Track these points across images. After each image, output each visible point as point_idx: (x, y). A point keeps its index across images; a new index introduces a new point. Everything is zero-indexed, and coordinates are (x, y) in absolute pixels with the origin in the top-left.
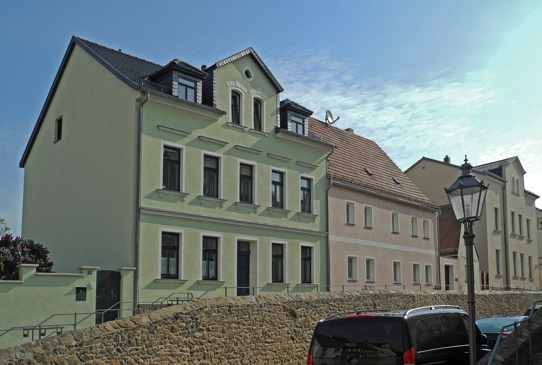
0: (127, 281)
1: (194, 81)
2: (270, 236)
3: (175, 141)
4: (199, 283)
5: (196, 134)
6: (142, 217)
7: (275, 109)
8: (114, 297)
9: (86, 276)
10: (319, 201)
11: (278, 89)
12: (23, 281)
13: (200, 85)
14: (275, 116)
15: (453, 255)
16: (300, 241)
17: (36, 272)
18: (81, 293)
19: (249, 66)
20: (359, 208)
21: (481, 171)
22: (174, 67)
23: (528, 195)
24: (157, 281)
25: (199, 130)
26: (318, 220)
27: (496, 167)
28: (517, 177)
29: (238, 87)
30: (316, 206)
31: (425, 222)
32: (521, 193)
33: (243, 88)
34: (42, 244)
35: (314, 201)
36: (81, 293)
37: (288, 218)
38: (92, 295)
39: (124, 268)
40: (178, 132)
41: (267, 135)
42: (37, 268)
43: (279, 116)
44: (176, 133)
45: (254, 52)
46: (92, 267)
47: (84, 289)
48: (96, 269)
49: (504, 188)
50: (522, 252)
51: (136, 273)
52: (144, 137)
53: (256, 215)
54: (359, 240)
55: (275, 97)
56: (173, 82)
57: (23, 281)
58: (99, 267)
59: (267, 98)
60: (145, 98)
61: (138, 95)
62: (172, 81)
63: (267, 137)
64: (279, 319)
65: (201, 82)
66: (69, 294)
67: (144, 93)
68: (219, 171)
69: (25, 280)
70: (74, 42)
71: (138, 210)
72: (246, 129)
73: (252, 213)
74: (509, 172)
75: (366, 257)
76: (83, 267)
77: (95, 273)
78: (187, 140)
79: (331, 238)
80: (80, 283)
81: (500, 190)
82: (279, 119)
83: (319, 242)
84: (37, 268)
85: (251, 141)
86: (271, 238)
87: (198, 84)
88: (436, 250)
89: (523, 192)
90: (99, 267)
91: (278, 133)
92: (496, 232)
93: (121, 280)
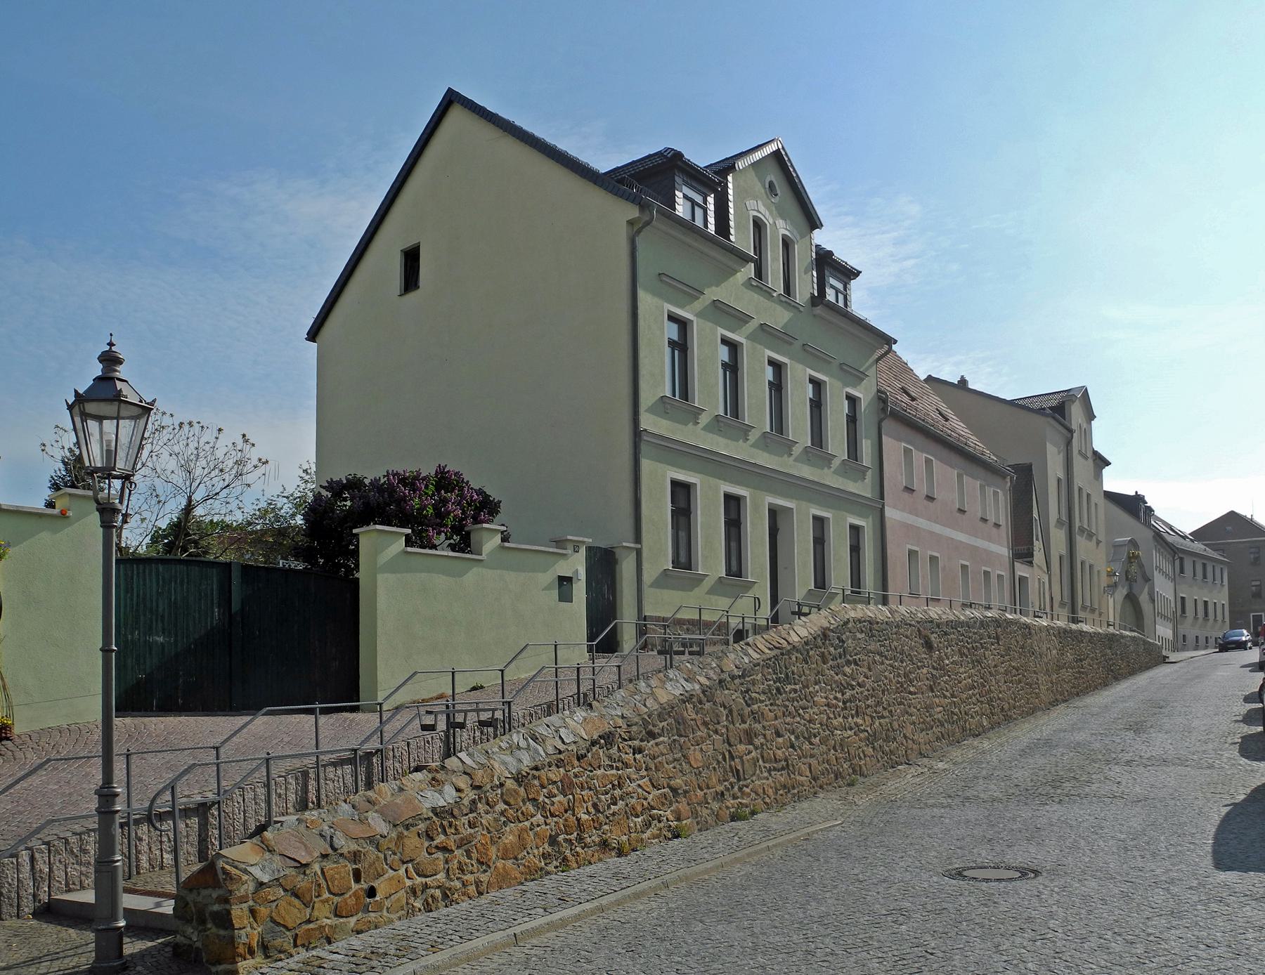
0: (626, 568)
1: (703, 193)
2: (810, 501)
3: (682, 307)
4: (721, 582)
5: (712, 293)
6: (644, 448)
7: (809, 260)
8: (609, 598)
9: (572, 555)
10: (869, 442)
11: (813, 222)
12: (484, 557)
13: (711, 199)
14: (810, 273)
15: (1025, 560)
16: (848, 514)
17: (502, 541)
18: (565, 582)
19: (773, 176)
20: (919, 457)
21: (1036, 406)
22: (679, 163)
23: (1098, 461)
24: (668, 573)
25: (714, 288)
26: (869, 473)
27: (1054, 403)
28: (1085, 425)
29: (760, 213)
30: (866, 447)
31: (996, 493)
32: (1089, 454)
33: (767, 214)
34: (1136, 492)
35: (864, 441)
36: (565, 582)
37: (832, 470)
38: (580, 590)
39: (624, 544)
40: (685, 289)
41: (801, 309)
42: (407, 536)
43: (815, 273)
44: (683, 290)
45: (783, 148)
46: (581, 539)
47: (569, 580)
48: (583, 542)
49: (1069, 443)
50: (1092, 562)
51: (639, 553)
52: (642, 294)
53: (792, 458)
54: (921, 520)
55: (808, 237)
56: (677, 192)
57: (484, 557)
58: (591, 540)
59: (798, 237)
60: (646, 218)
61: (633, 212)
62: (674, 189)
63: (801, 312)
64: (916, 651)
65: (713, 195)
66: (547, 588)
67: (643, 206)
68: (738, 369)
69: (487, 555)
70: (451, 99)
71: (637, 433)
72: (775, 295)
73: (786, 456)
74: (1076, 411)
75: (930, 553)
76: (569, 537)
77: (583, 551)
78: (699, 305)
79: (889, 512)
80: (564, 569)
81: (1063, 447)
82: (815, 280)
83: (871, 518)
84: (407, 536)
85: (779, 317)
86: (812, 505)
87: (709, 198)
88: (1008, 548)
89: (1091, 452)
90: (591, 540)
91: (818, 306)
92: (1060, 523)
93: (617, 567)
